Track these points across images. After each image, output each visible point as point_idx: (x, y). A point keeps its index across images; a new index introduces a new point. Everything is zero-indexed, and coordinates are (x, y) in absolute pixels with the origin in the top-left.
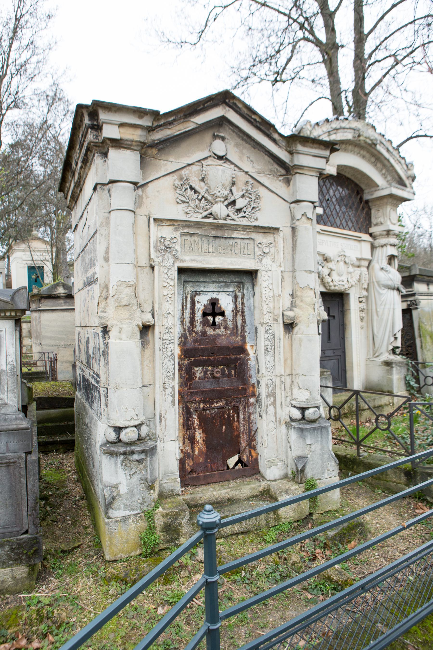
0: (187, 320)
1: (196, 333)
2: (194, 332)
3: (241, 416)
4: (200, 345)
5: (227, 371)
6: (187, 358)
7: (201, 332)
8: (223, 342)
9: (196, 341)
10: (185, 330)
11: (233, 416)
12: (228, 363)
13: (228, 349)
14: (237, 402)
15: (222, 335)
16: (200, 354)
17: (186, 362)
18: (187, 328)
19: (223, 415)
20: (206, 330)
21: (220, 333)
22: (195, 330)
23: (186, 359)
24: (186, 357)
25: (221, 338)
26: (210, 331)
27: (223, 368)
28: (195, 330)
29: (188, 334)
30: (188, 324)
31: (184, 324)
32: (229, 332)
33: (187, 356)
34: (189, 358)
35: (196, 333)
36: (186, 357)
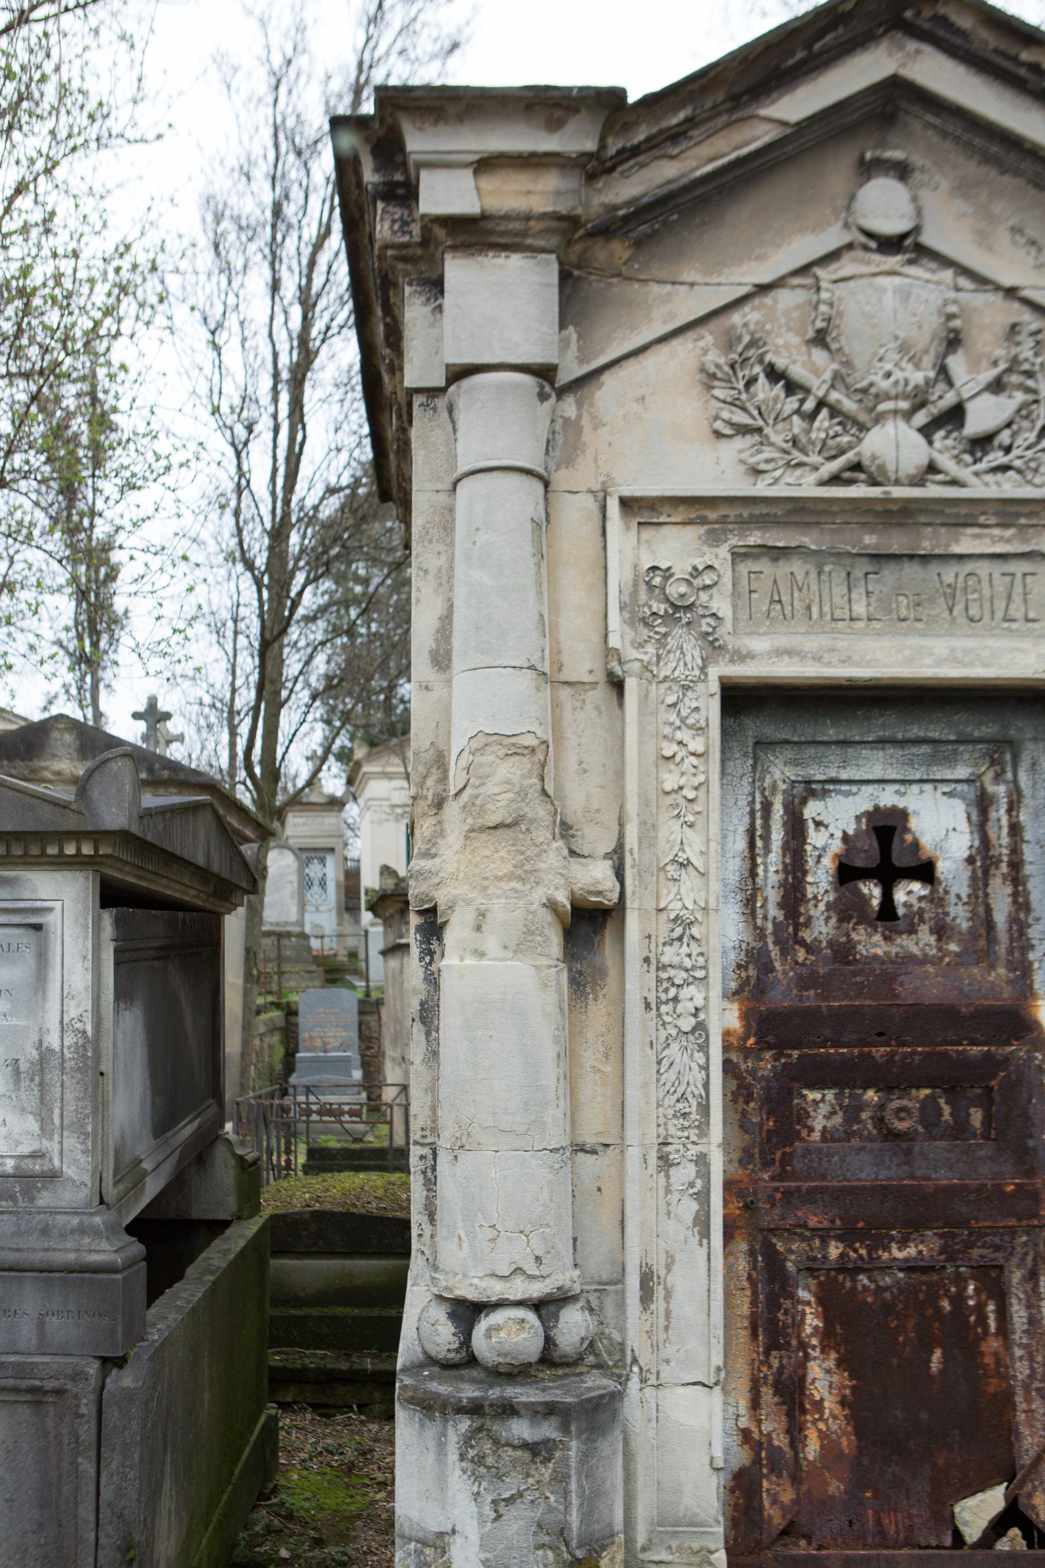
0: (772, 896)
1: (809, 949)
2: (802, 943)
3: (1019, 1314)
4: (827, 999)
5: (947, 1110)
6: (770, 1047)
7: (830, 944)
8: (929, 987)
9: (807, 980)
10: (760, 933)
11: (980, 1308)
12: (954, 1080)
13: (948, 1019)
14: (997, 1248)
15: (925, 960)
16: (827, 1032)
17: (767, 1065)
18: (770, 927)
19: (933, 1299)
20: (855, 936)
21: (915, 950)
22: (807, 935)
23: (768, 1055)
24: (764, 1044)
25: (918, 970)
26: (871, 944)
27: (932, 1099)
28: (807, 935)
29: (775, 952)
30: (774, 912)
31: (760, 913)
32: (953, 947)
33: (771, 1039)
34: (780, 1047)
35: (809, 949)
36: (764, 1044)
